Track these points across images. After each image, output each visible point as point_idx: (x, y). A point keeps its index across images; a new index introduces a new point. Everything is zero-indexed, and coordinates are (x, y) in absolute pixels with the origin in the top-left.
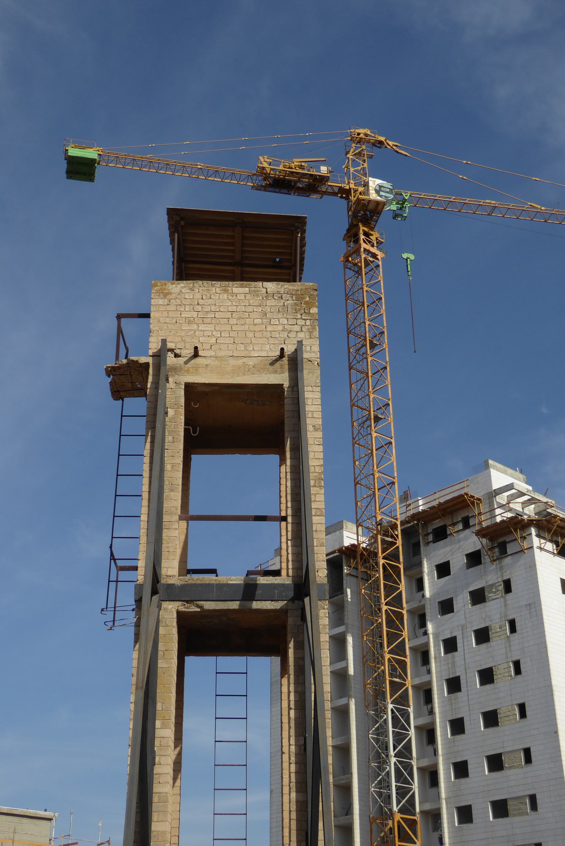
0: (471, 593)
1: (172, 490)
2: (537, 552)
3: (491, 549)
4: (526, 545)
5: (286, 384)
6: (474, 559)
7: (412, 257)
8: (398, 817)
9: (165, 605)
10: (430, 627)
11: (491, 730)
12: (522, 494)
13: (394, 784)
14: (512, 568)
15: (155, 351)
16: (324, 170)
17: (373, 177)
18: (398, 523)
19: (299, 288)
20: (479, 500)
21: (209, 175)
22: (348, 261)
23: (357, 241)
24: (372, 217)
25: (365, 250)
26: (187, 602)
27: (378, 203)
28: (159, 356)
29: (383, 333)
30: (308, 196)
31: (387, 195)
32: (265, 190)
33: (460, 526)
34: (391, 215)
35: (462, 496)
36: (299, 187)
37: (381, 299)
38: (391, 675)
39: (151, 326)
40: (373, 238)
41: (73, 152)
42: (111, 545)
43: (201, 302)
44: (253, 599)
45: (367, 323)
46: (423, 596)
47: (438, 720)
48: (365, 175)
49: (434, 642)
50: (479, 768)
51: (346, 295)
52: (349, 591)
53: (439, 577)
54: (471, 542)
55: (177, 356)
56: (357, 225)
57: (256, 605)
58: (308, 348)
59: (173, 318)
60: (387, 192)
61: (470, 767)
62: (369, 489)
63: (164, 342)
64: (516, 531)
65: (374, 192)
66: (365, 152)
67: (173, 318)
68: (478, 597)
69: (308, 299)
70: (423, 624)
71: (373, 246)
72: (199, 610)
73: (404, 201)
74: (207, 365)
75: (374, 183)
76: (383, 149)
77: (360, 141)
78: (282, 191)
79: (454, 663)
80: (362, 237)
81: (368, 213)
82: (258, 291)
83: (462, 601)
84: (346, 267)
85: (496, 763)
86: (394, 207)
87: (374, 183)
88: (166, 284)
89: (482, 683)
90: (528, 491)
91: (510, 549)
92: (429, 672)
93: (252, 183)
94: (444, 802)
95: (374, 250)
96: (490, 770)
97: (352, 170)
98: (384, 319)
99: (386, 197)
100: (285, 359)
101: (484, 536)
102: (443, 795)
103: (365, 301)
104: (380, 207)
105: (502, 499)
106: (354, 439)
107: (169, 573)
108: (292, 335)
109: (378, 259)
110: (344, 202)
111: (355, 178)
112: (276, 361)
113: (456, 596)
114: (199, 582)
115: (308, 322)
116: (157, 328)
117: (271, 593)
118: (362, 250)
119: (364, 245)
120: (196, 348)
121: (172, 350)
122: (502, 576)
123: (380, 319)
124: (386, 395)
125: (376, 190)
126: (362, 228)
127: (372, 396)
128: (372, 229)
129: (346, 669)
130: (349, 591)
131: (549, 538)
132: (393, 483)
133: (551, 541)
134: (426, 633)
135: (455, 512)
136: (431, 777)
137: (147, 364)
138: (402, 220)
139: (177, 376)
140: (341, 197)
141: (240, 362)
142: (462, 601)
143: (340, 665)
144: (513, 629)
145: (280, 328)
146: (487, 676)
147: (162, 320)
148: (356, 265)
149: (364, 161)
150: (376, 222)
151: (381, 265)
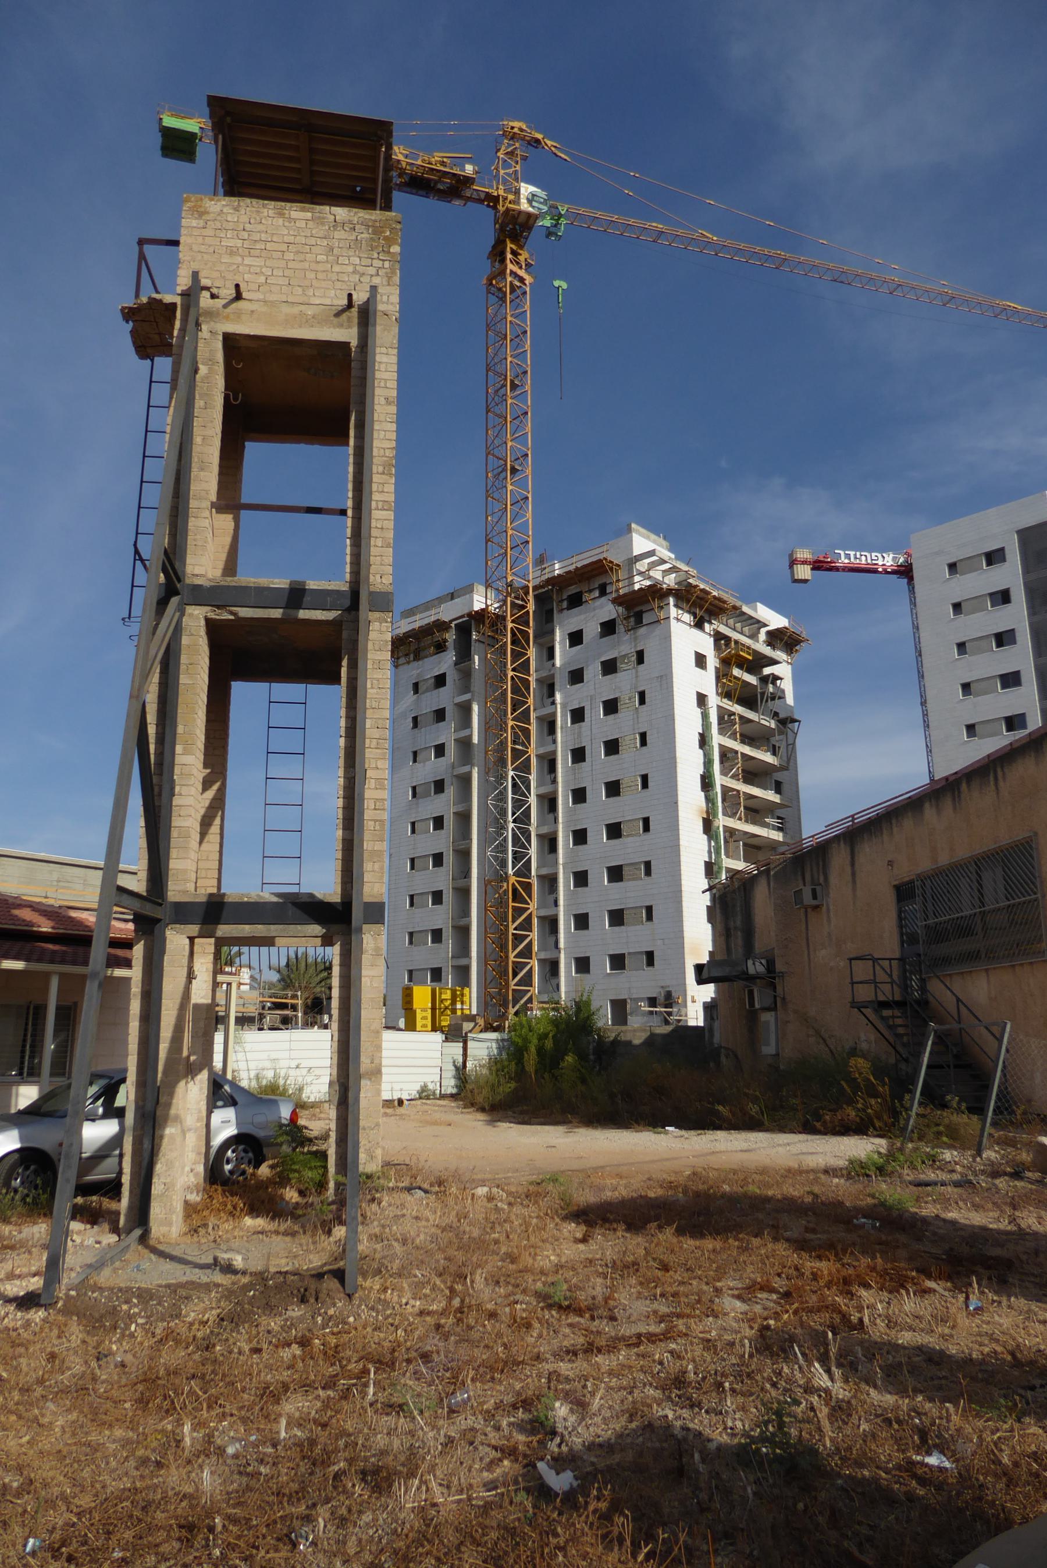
0: (605, 664)
1: (202, 469)
2: (673, 622)
3: (627, 618)
4: (662, 615)
5: (354, 343)
6: (608, 628)
7: (565, 286)
8: (513, 879)
9: (190, 610)
10: (558, 697)
11: (612, 799)
12: (664, 562)
13: (510, 848)
14: (647, 639)
15: (185, 288)
16: (469, 169)
17: (527, 182)
18: (531, 585)
19: (378, 218)
20: (618, 566)
22: (491, 284)
23: (503, 261)
25: (511, 271)
26: (218, 607)
27: (529, 215)
28: (190, 296)
29: (526, 372)
30: (450, 202)
31: (541, 206)
33: (597, 594)
34: (544, 232)
35: (600, 561)
36: (439, 191)
37: (526, 332)
38: (514, 742)
39: (181, 255)
40: (522, 258)
41: (170, 121)
42: (136, 542)
43: (248, 227)
44: (299, 606)
45: (509, 359)
46: (554, 665)
47: (560, 789)
48: (517, 180)
49: (562, 712)
50: (598, 836)
51: (488, 325)
52: (476, 657)
53: (570, 646)
54: (606, 610)
55: (213, 296)
57: (303, 614)
58: (385, 298)
59: (210, 246)
61: (588, 834)
62: (502, 547)
63: (195, 275)
64: (654, 600)
66: (518, 152)
67: (210, 246)
68: (610, 667)
69: (388, 233)
70: (552, 694)
71: (521, 268)
72: (232, 617)
73: (560, 216)
74: (252, 312)
75: (526, 189)
76: (540, 149)
77: (513, 137)
78: (421, 192)
79: (580, 734)
80: (509, 256)
81: (517, 227)
82: (324, 218)
83: (593, 671)
84: (488, 292)
85: (614, 831)
86: (547, 222)
88: (201, 199)
89: (607, 754)
90: (670, 558)
91: (647, 618)
92: (554, 742)
94: (561, 867)
95: (522, 273)
96: (608, 839)
97: (502, 172)
100: (354, 311)
101: (620, 604)
102: (561, 861)
105: (642, 565)
106: (487, 491)
107: (196, 572)
108: (366, 279)
110: (491, 212)
111: (505, 182)
112: (343, 311)
113: (588, 666)
114: (234, 584)
115: (387, 264)
116: (187, 258)
117: (322, 599)
118: (508, 271)
119: (510, 266)
120: (237, 286)
121: (207, 289)
122: (635, 646)
123: (522, 356)
124: (526, 445)
125: (528, 199)
126: (510, 245)
127: (509, 444)
128: (521, 247)
129: (470, 737)
130: (476, 657)
131: (687, 608)
132: (527, 542)
133: (689, 612)
134: (553, 703)
135: (594, 577)
136: (550, 843)
137: (174, 305)
139: (212, 323)
140: (488, 206)
141: (296, 310)
142: (593, 671)
143: (464, 733)
144: (642, 701)
145: (350, 269)
146: (612, 747)
147: (195, 248)
148: (500, 289)
149: (517, 163)
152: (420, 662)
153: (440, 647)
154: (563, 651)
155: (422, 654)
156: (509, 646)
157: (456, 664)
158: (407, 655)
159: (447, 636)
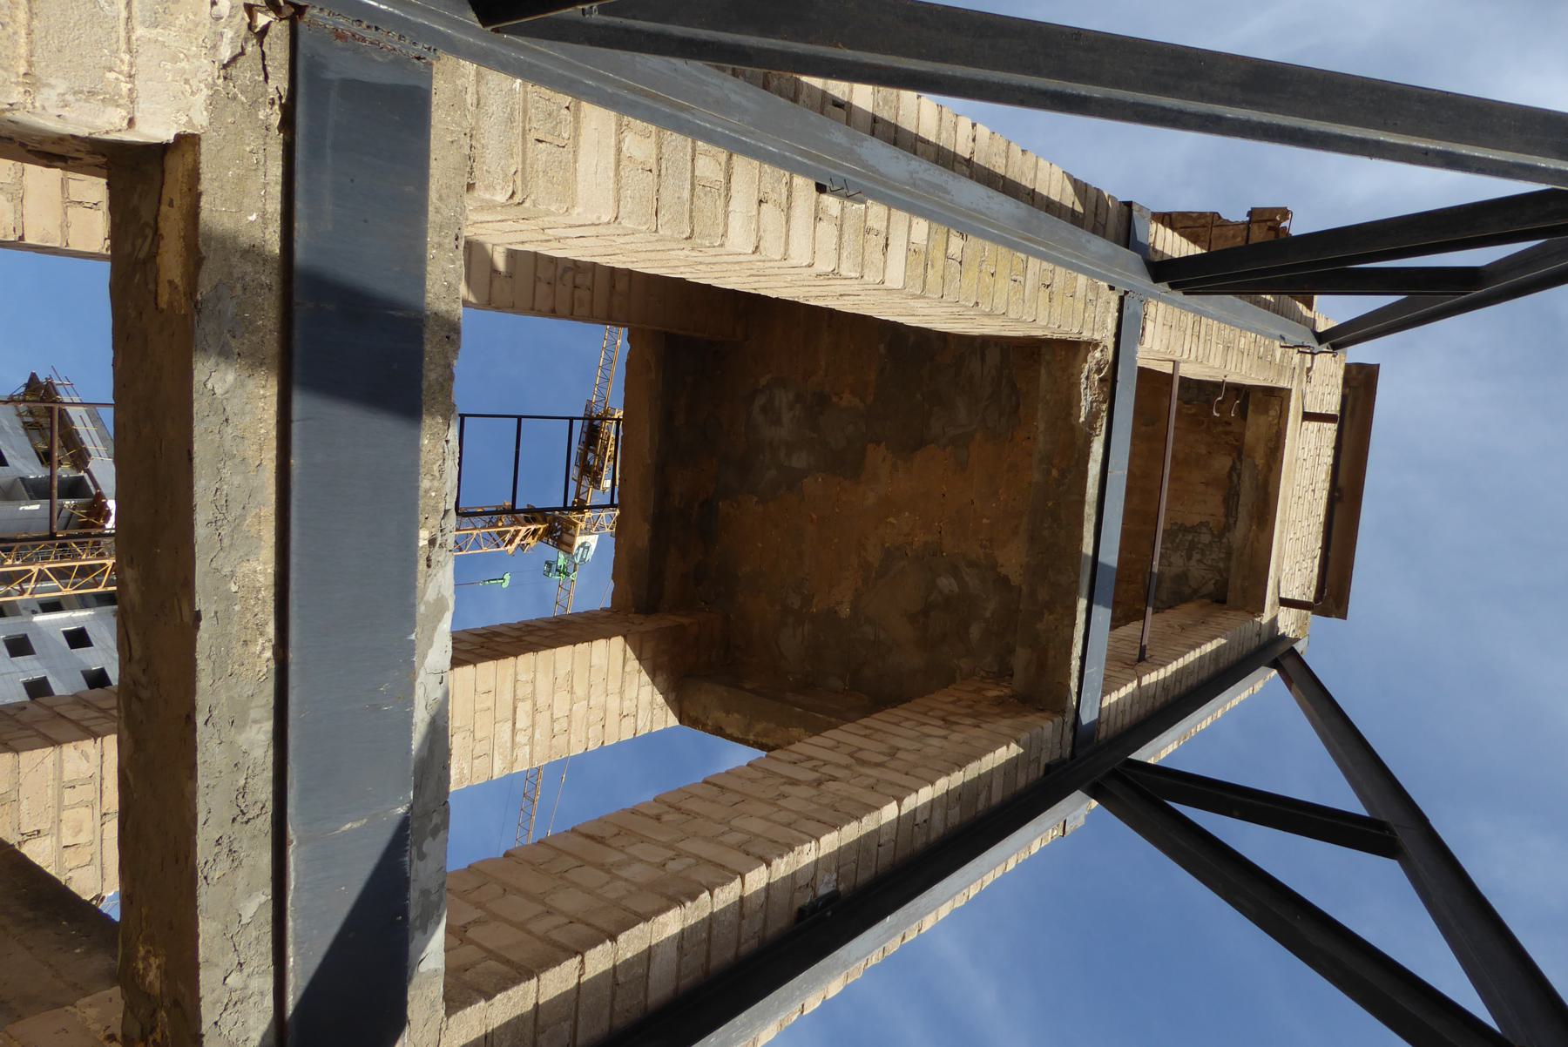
0: (44, 681)
7: (505, 585)
23: (528, 521)
25: (517, 532)
27: (571, 545)
34: (551, 559)
40: (530, 540)
46: (35, 612)
52: (37, 507)
53: (65, 633)
56: (545, 521)
73: (567, 574)
75: (592, 540)
80: (533, 527)
86: (561, 563)
87: (592, 540)
95: (517, 541)
119: (524, 529)
126: (542, 527)
128: (540, 539)
130: (37, 507)
142: (28, 667)
152: (22, 432)
153: (46, 458)
154: (57, 623)
155: (35, 433)
156: (77, 564)
157: (23, 479)
158: (31, 412)
159: (66, 467)
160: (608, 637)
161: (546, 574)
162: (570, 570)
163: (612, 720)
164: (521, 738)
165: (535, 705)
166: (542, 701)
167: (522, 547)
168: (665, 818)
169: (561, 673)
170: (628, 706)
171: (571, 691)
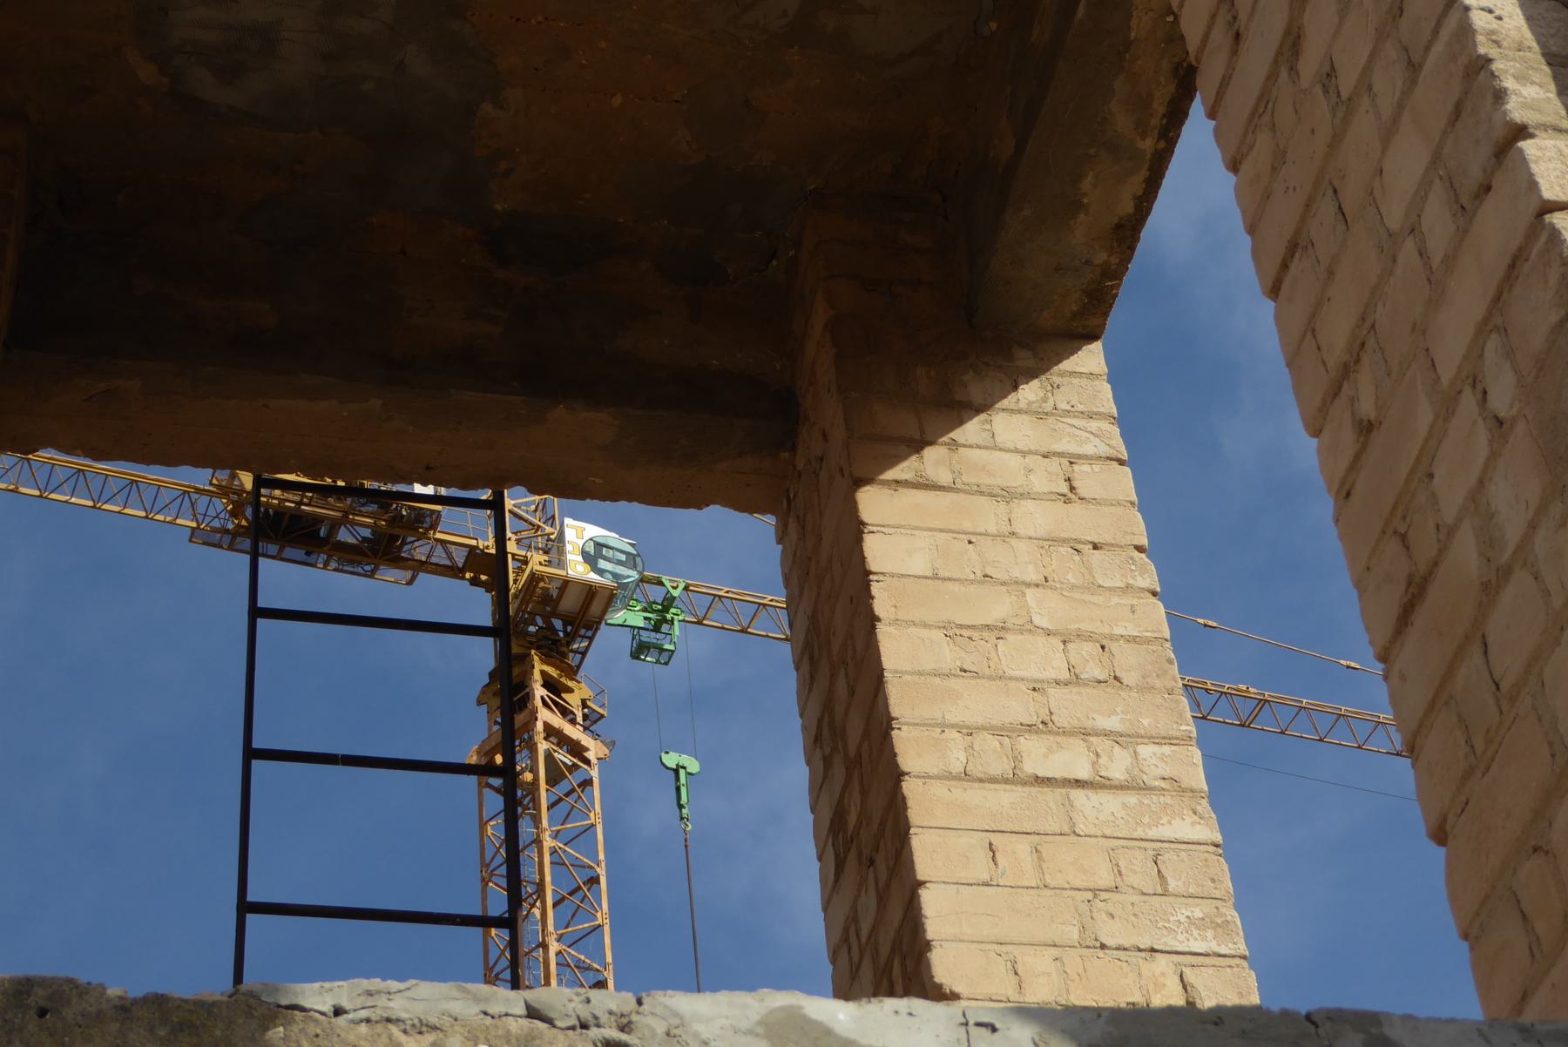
7: (693, 766)
21: (51, 487)
24: (571, 637)
25: (548, 728)
27: (590, 591)
32: (231, 548)
34: (626, 642)
36: (343, 547)
37: (594, 880)
40: (573, 700)
45: (554, 947)
48: (551, 520)
56: (525, 659)
60: (619, 563)
65: (580, 558)
71: (573, 722)
73: (669, 602)
75: (579, 533)
78: (289, 552)
80: (539, 692)
81: (558, 624)
86: (636, 619)
93: (195, 518)
98: (607, 941)
99: (615, 576)
103: (548, 878)
104: (595, 608)
109: (587, 762)
118: (540, 726)
119: (544, 715)
125: (585, 554)
126: (539, 667)
128: (572, 672)
138: (658, 662)
140: (475, 582)
150: (584, 654)
151: (596, 781)
160: (857, 529)
161: (664, 656)
162: (656, 594)
163: (1081, 522)
164: (1117, 766)
165: (1030, 728)
166: (1020, 709)
167: (591, 721)
168: (1367, 408)
169: (948, 655)
170: (1045, 478)
171: (999, 630)
